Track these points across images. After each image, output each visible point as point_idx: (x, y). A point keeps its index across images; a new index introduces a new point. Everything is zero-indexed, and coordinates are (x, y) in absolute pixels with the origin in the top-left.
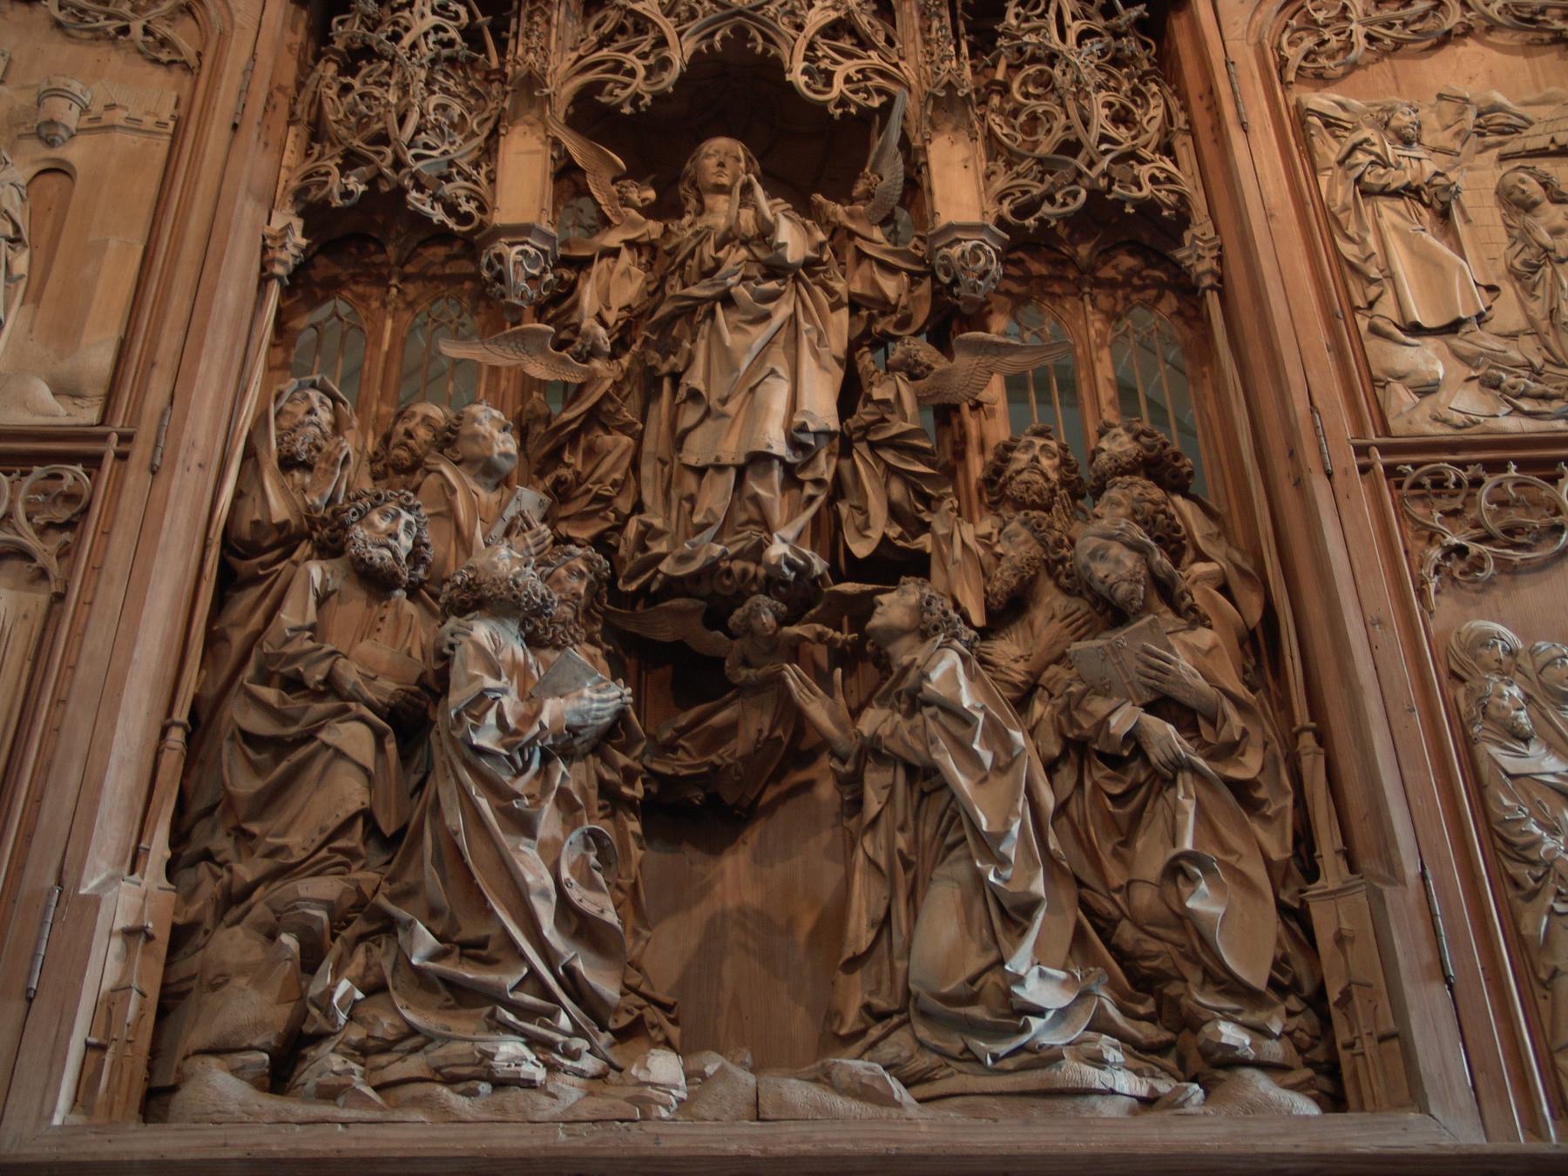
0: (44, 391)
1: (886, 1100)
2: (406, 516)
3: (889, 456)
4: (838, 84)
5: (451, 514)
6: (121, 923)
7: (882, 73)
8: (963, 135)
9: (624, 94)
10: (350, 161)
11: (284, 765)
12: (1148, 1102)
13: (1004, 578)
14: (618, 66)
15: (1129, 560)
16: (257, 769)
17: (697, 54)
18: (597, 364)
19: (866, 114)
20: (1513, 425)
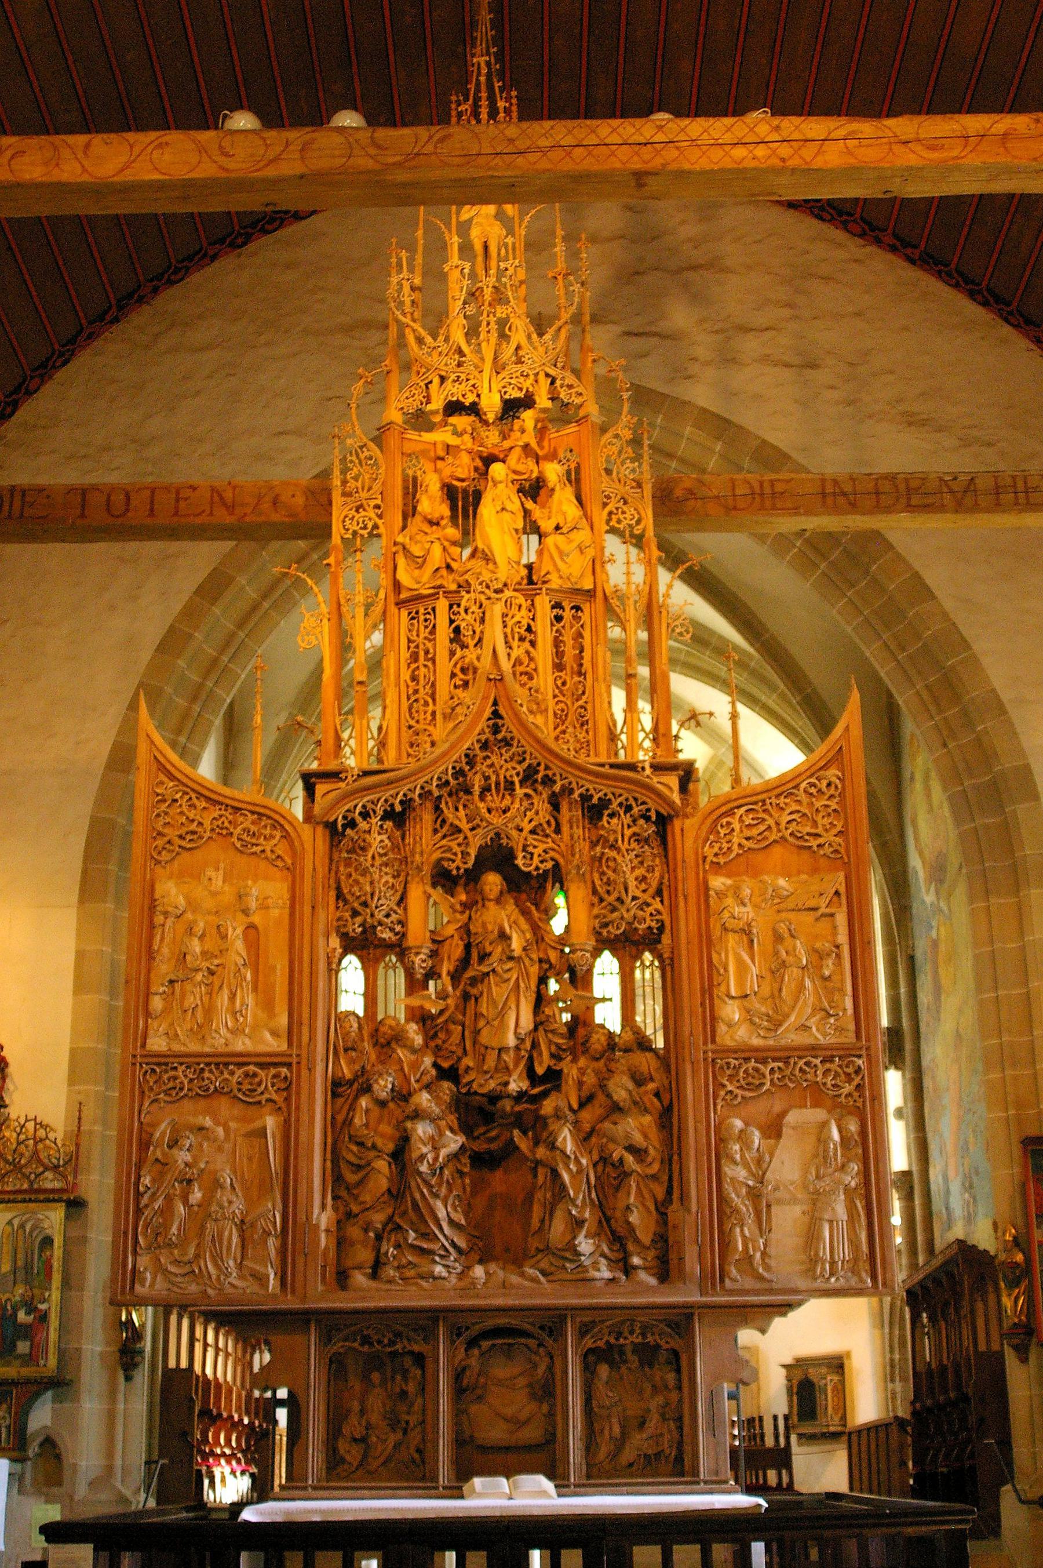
0: (268, 1036)
1: (538, 1282)
2: (390, 1079)
3: (550, 1035)
4: (536, 860)
5: (402, 1069)
6: (323, 1227)
7: (553, 850)
8: (582, 885)
9: (454, 865)
10: (355, 913)
11: (362, 1174)
12: (612, 1280)
13: (585, 1092)
14: (450, 849)
15: (623, 1094)
16: (353, 1172)
17: (481, 847)
18: (449, 1001)
19: (546, 872)
20: (756, 1042)
